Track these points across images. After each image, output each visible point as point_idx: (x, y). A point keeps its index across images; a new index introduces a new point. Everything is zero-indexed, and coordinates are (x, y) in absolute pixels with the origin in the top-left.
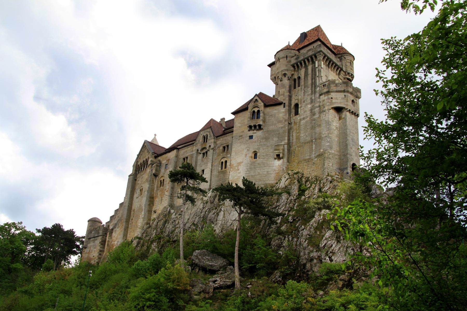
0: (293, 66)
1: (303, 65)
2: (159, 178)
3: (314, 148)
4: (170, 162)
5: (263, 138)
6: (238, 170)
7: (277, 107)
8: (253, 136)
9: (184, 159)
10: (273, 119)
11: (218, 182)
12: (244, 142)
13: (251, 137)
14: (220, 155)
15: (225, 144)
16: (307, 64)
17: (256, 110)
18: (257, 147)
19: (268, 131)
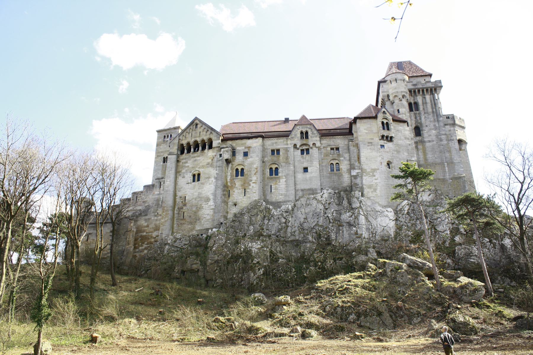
0: (410, 91)
1: (421, 93)
2: (235, 166)
3: (447, 170)
4: (251, 149)
5: (394, 151)
6: (375, 176)
7: (402, 124)
8: (384, 146)
9: (273, 151)
10: (400, 134)
11: (331, 184)
12: (376, 150)
13: (382, 146)
14: (329, 156)
15: (334, 145)
16: (425, 93)
17: (385, 121)
18: (390, 158)
19: (398, 145)
